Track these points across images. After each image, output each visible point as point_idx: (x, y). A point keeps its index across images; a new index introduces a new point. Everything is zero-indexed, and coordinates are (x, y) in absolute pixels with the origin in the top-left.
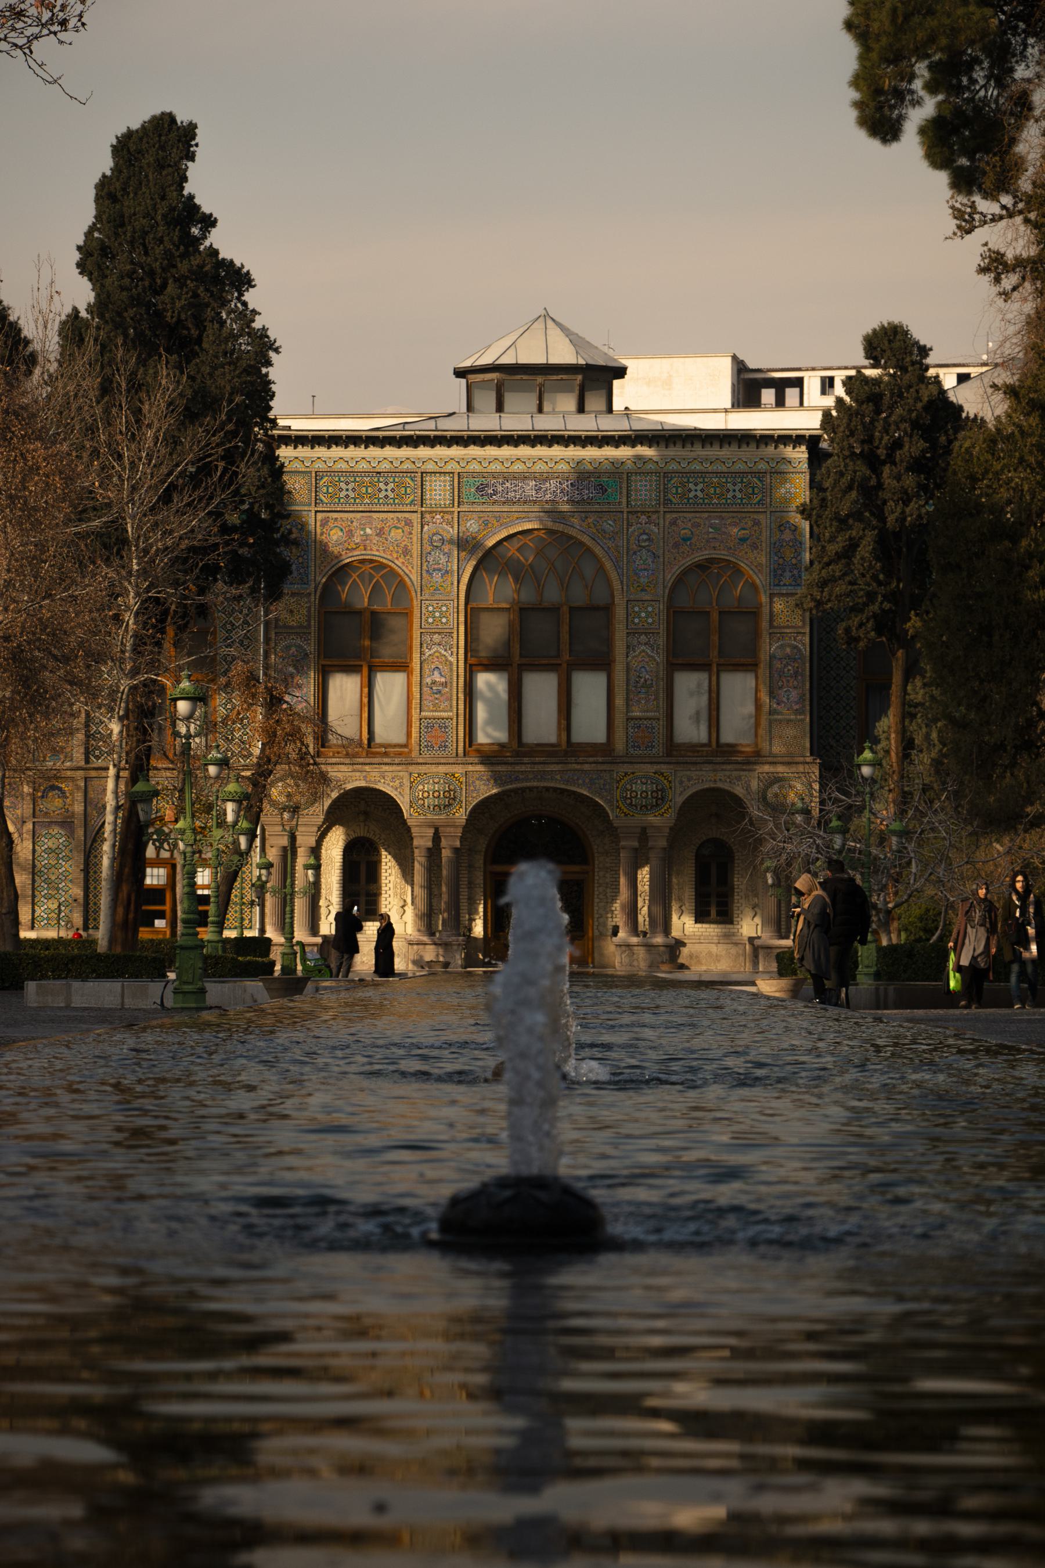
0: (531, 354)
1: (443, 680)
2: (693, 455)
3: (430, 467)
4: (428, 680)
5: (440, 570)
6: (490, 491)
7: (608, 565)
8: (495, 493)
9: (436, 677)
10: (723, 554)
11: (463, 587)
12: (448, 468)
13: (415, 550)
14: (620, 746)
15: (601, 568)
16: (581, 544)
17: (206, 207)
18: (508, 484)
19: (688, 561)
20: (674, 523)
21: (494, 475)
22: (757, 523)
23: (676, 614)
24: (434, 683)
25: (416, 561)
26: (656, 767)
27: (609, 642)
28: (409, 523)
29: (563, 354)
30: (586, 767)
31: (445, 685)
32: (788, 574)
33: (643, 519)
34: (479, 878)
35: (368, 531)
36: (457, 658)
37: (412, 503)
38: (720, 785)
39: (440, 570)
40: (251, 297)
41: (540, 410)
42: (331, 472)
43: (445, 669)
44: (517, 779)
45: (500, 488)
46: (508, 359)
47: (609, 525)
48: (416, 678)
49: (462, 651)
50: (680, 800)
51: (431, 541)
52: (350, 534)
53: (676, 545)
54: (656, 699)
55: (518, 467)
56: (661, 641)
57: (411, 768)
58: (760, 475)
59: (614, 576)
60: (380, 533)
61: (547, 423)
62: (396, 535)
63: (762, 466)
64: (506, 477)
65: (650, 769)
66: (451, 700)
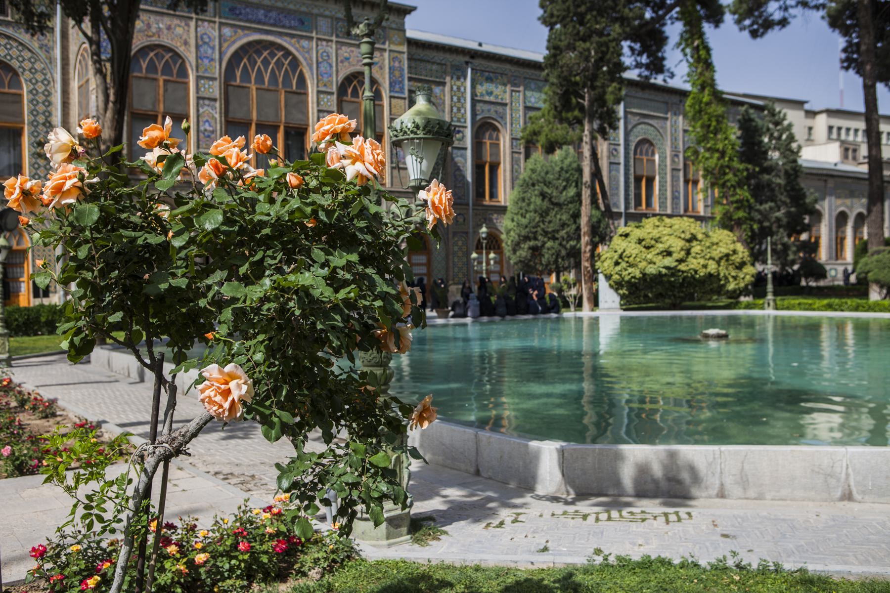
1: (211, 129)
5: (207, 58)
6: (238, 12)
8: (240, 14)
9: (207, 127)
13: (192, 42)
18: (248, 10)
24: (206, 130)
25: (193, 49)
32: (397, 86)
35: (161, 26)
39: (207, 58)
45: (243, 12)
47: (305, 43)
51: (202, 38)
52: (149, 26)
60: (169, 28)
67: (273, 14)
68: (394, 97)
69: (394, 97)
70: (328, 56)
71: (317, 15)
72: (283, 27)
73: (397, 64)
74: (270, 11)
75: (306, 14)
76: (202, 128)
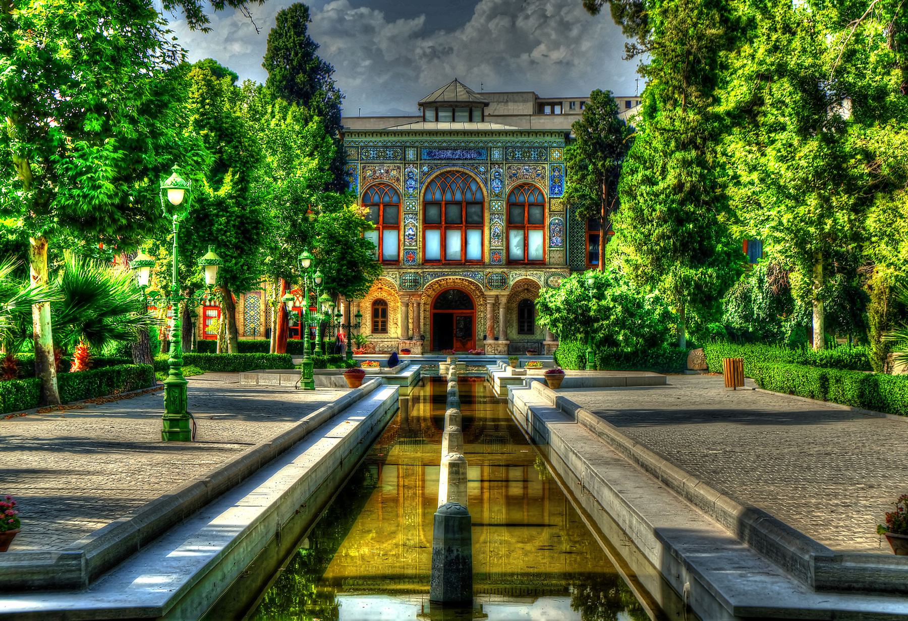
0: (449, 96)
2: (517, 140)
3: (408, 144)
4: (407, 233)
7: (482, 185)
8: (435, 155)
9: (411, 232)
10: (530, 181)
11: (422, 194)
12: (417, 144)
13: (402, 179)
14: (487, 260)
15: (480, 186)
16: (471, 177)
17: (315, 39)
19: (515, 184)
20: (509, 168)
21: (435, 148)
22: (544, 168)
23: (511, 205)
26: (502, 270)
27: (482, 217)
28: (399, 168)
29: (462, 96)
30: (473, 270)
31: (414, 235)
32: (557, 189)
33: (497, 166)
35: (382, 171)
36: (420, 226)
37: (400, 159)
38: (528, 277)
40: (334, 77)
41: (454, 121)
42: (366, 147)
43: (414, 229)
44: (444, 275)
46: (439, 99)
48: (402, 233)
49: (421, 221)
50: (512, 283)
51: (408, 175)
52: (375, 172)
53: (510, 177)
54: (502, 241)
55: (445, 144)
56: (504, 217)
57: (400, 270)
58: (546, 148)
59: (484, 190)
60: (387, 172)
62: (394, 173)
63: (546, 144)
64: (440, 149)
65: (499, 271)
66: (416, 241)
67: (459, 152)
68: (554, 198)
69: (554, 198)
70: (499, 175)
71: (491, 148)
72: (466, 159)
73: (557, 174)
74: (457, 150)
75: (483, 148)
76: (407, 233)
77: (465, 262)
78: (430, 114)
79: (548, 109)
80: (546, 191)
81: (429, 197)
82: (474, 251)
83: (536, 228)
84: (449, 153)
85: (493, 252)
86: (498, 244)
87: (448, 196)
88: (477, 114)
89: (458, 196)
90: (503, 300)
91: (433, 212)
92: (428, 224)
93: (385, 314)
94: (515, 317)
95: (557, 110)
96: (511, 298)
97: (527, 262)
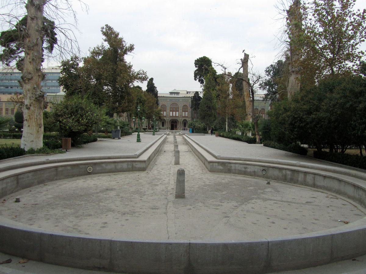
17: (154, 83)
29: (176, 92)
34: (170, 124)
40: (157, 89)
61: (175, 96)
77: (176, 116)
78: (171, 94)
79: (189, 93)
80: (188, 106)
81: (171, 107)
82: (177, 115)
83: (187, 111)
84: (174, 100)
85: (180, 115)
86: (181, 114)
87: (174, 107)
88: (178, 94)
89: (175, 107)
90: (181, 122)
91: (171, 109)
92: (170, 111)
93: (164, 124)
94: (183, 125)
95: (190, 93)
96: (183, 122)
97: (185, 117)
